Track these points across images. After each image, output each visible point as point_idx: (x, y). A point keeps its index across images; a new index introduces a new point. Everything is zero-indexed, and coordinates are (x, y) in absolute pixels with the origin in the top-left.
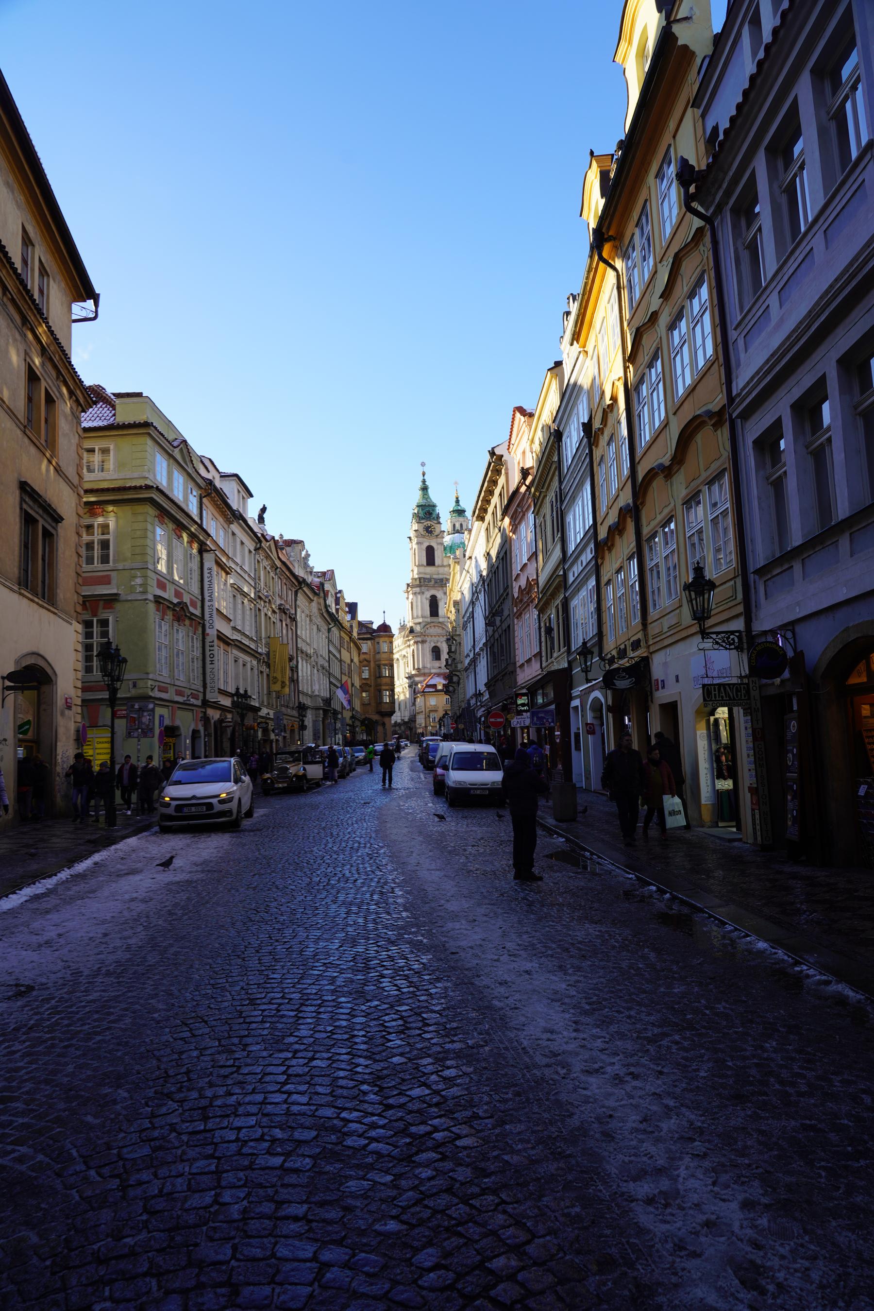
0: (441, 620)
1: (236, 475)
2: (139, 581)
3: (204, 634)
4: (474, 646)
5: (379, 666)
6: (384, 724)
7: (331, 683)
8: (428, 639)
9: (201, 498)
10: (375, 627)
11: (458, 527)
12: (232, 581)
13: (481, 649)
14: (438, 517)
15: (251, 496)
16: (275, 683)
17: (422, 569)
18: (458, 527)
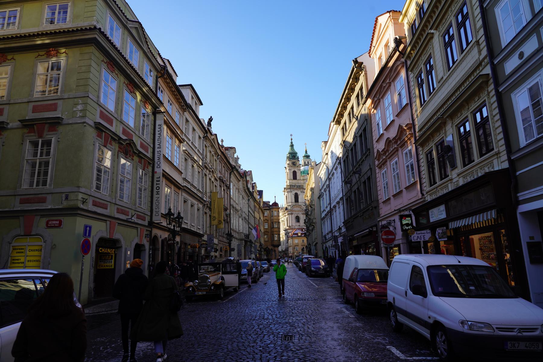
0: (300, 204)
1: (191, 85)
2: (80, 107)
3: (153, 172)
4: (330, 204)
5: (273, 223)
6: (275, 251)
7: (249, 227)
8: (294, 213)
9: (157, 78)
10: (271, 204)
11: (307, 163)
12: (184, 149)
13: (338, 203)
14: (298, 158)
15: (202, 104)
16: (214, 220)
17: (291, 181)
18: (307, 163)
